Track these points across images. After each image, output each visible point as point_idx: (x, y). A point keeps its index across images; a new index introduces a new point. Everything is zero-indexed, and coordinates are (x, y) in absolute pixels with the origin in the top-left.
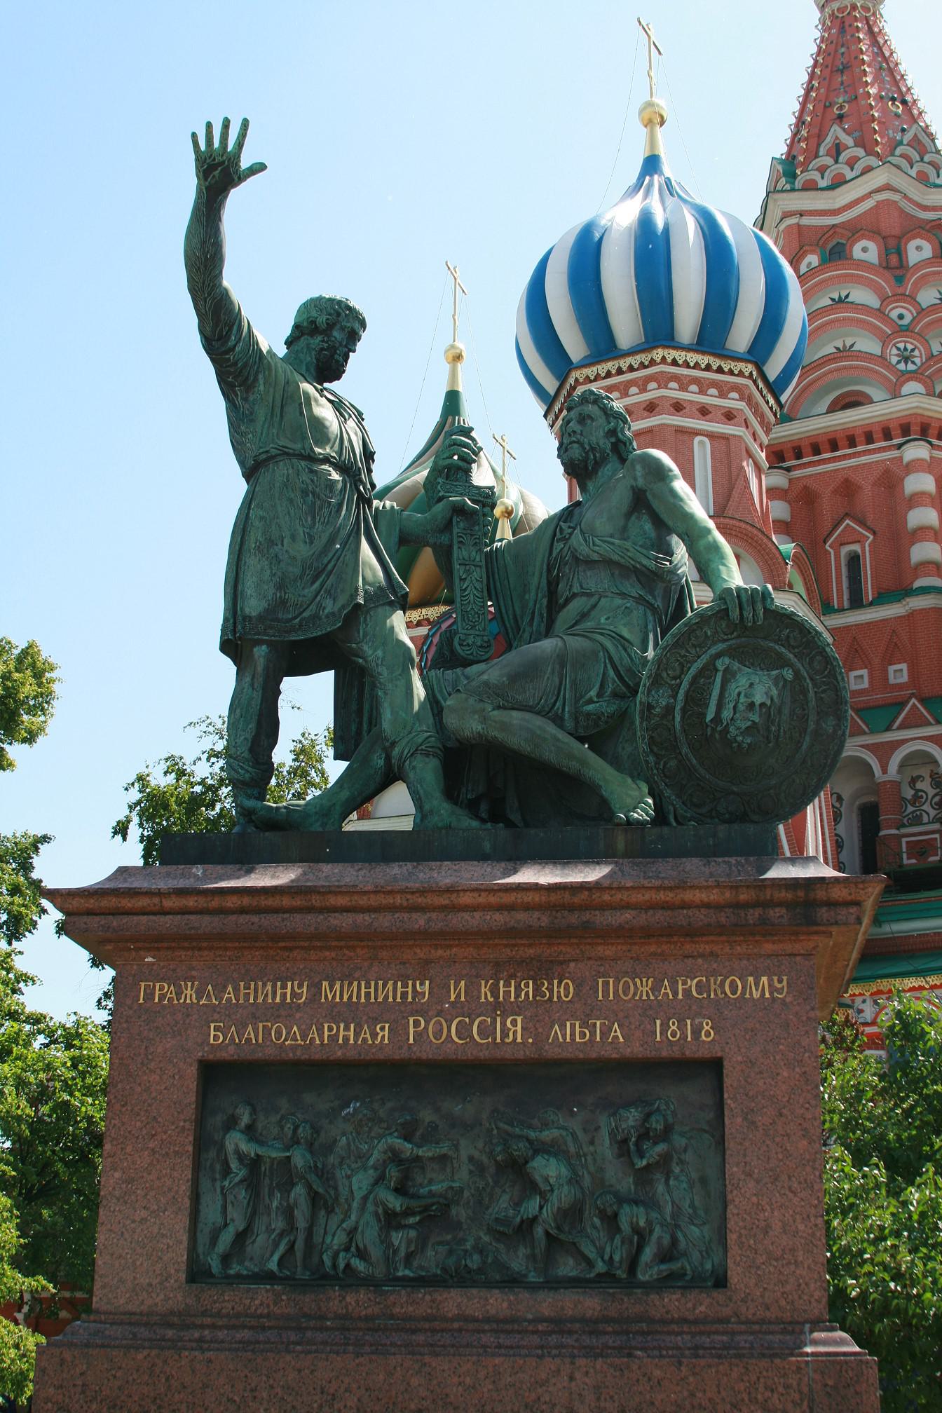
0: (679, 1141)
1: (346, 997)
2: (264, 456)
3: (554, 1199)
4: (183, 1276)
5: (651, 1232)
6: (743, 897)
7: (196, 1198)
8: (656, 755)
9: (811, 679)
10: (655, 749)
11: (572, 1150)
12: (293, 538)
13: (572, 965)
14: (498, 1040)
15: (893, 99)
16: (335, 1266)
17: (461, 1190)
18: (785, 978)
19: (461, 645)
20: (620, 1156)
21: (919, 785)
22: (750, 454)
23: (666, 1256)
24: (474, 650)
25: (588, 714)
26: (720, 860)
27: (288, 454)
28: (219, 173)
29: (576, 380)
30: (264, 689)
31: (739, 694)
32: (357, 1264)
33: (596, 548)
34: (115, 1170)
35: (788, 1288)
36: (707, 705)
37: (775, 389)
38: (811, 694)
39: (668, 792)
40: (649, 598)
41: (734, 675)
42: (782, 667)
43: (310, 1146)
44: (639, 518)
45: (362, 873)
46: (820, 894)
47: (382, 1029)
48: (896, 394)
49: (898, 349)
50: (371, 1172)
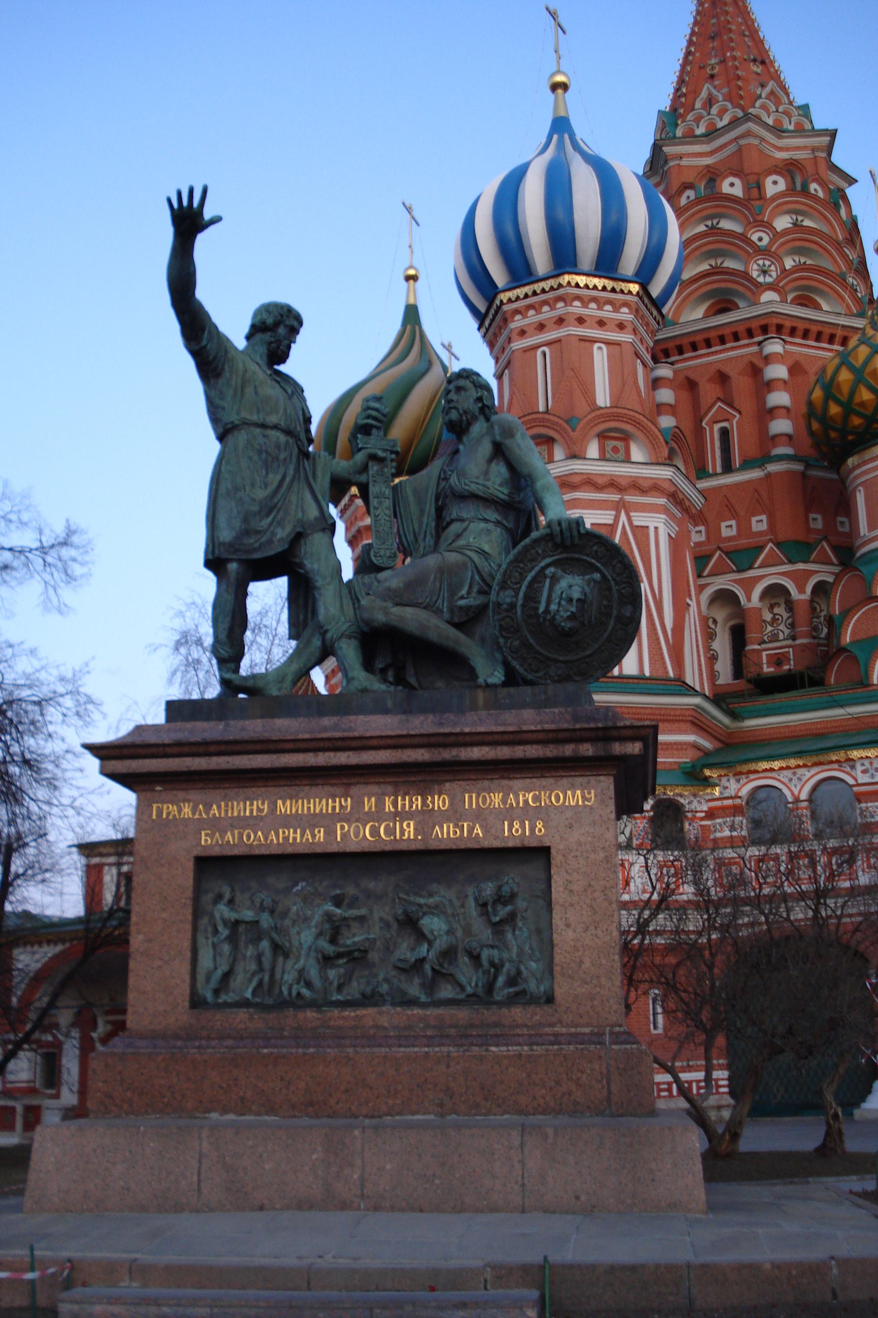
0: (521, 904)
1: (294, 811)
2: (230, 426)
3: (437, 944)
4: (187, 1004)
5: (503, 966)
6: (561, 736)
7: (195, 951)
8: (504, 637)
9: (614, 580)
10: (504, 634)
11: (449, 911)
12: (253, 485)
13: (447, 785)
14: (398, 837)
15: (754, 61)
16: (290, 994)
17: (375, 939)
18: (593, 791)
19: (375, 556)
20: (482, 915)
21: (776, 610)
22: (637, 355)
23: (512, 981)
25: (461, 608)
26: (547, 710)
27: (247, 424)
28: (188, 221)
29: (501, 301)
31: (562, 593)
32: (305, 992)
33: (467, 487)
34: (139, 933)
35: (596, 1002)
36: (539, 602)
37: (657, 304)
38: (615, 588)
39: (514, 663)
40: (505, 522)
41: (558, 581)
42: (593, 573)
43: (272, 912)
45: (303, 725)
46: (614, 733)
47: (319, 832)
49: (759, 265)
50: (313, 930)
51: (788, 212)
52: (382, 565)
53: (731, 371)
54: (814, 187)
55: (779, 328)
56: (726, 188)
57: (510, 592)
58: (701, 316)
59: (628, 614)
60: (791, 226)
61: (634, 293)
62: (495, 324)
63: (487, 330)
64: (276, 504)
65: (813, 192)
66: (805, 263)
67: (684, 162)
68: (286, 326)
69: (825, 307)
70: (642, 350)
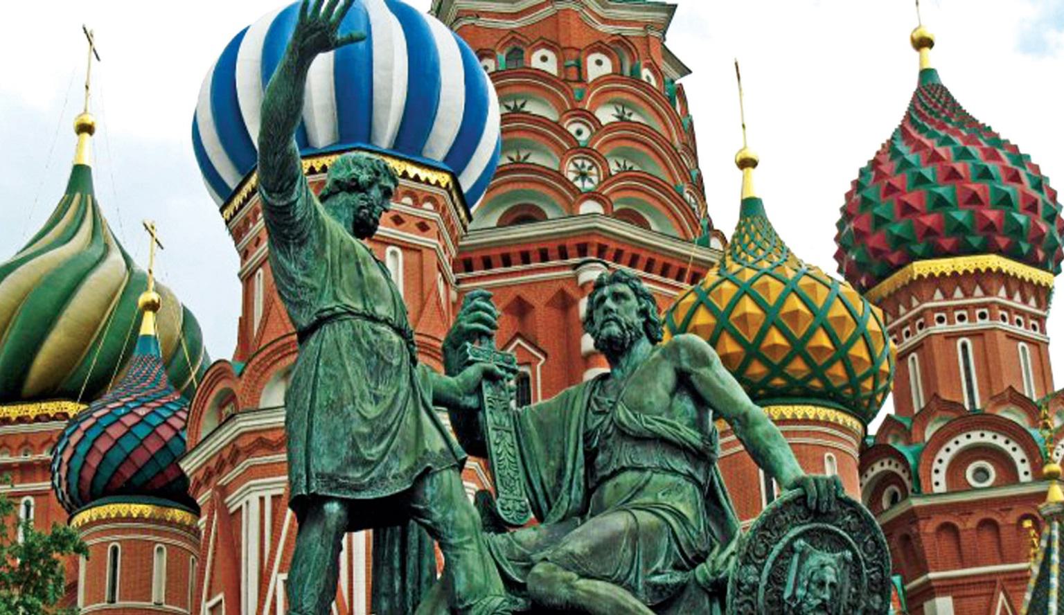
12: (362, 396)
19: (503, 509)
24: (514, 514)
25: (655, 586)
30: (334, 546)
33: (650, 426)
36: (784, 584)
41: (807, 558)
42: (843, 549)
44: (681, 400)
48: (573, 214)
49: (576, 165)
51: (614, 102)
52: (511, 521)
53: (538, 301)
54: (645, 73)
55: (601, 251)
56: (535, 61)
57: (752, 569)
58: (494, 224)
59: (877, 607)
60: (616, 119)
61: (443, 185)
62: (248, 206)
63: (236, 212)
64: (391, 426)
65: (645, 79)
66: (631, 168)
67: (482, 22)
68: (381, 187)
69: (654, 227)
70: (446, 258)
